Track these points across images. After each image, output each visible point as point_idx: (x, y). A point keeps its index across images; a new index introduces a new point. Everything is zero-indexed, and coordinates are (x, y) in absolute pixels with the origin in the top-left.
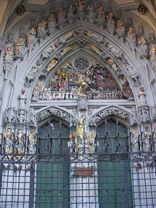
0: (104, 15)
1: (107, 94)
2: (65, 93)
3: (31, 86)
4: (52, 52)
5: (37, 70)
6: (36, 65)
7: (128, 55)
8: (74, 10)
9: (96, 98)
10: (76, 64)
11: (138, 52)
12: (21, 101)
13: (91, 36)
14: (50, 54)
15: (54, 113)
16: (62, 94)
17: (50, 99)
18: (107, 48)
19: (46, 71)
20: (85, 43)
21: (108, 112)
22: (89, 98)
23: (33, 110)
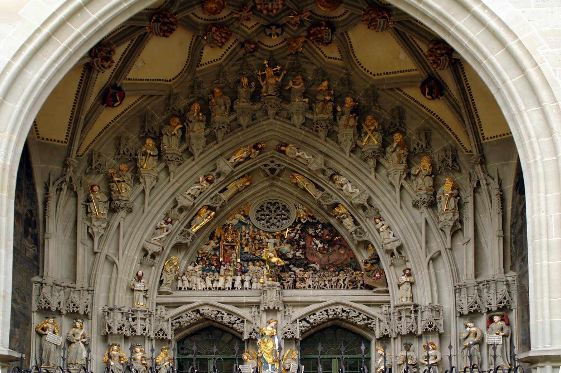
0: (330, 104)
1: (328, 278)
2: (234, 277)
3: (156, 265)
4: (201, 193)
5: (167, 233)
6: (165, 223)
7: (384, 199)
8: (253, 90)
9: (302, 286)
10: (259, 215)
11: (407, 191)
12: (136, 294)
13: (294, 156)
14: (195, 198)
15: (210, 314)
16: (226, 279)
17: (200, 288)
18: (334, 183)
19: (189, 234)
20: (281, 170)
21: (327, 314)
22: (286, 287)
23: (163, 310)
